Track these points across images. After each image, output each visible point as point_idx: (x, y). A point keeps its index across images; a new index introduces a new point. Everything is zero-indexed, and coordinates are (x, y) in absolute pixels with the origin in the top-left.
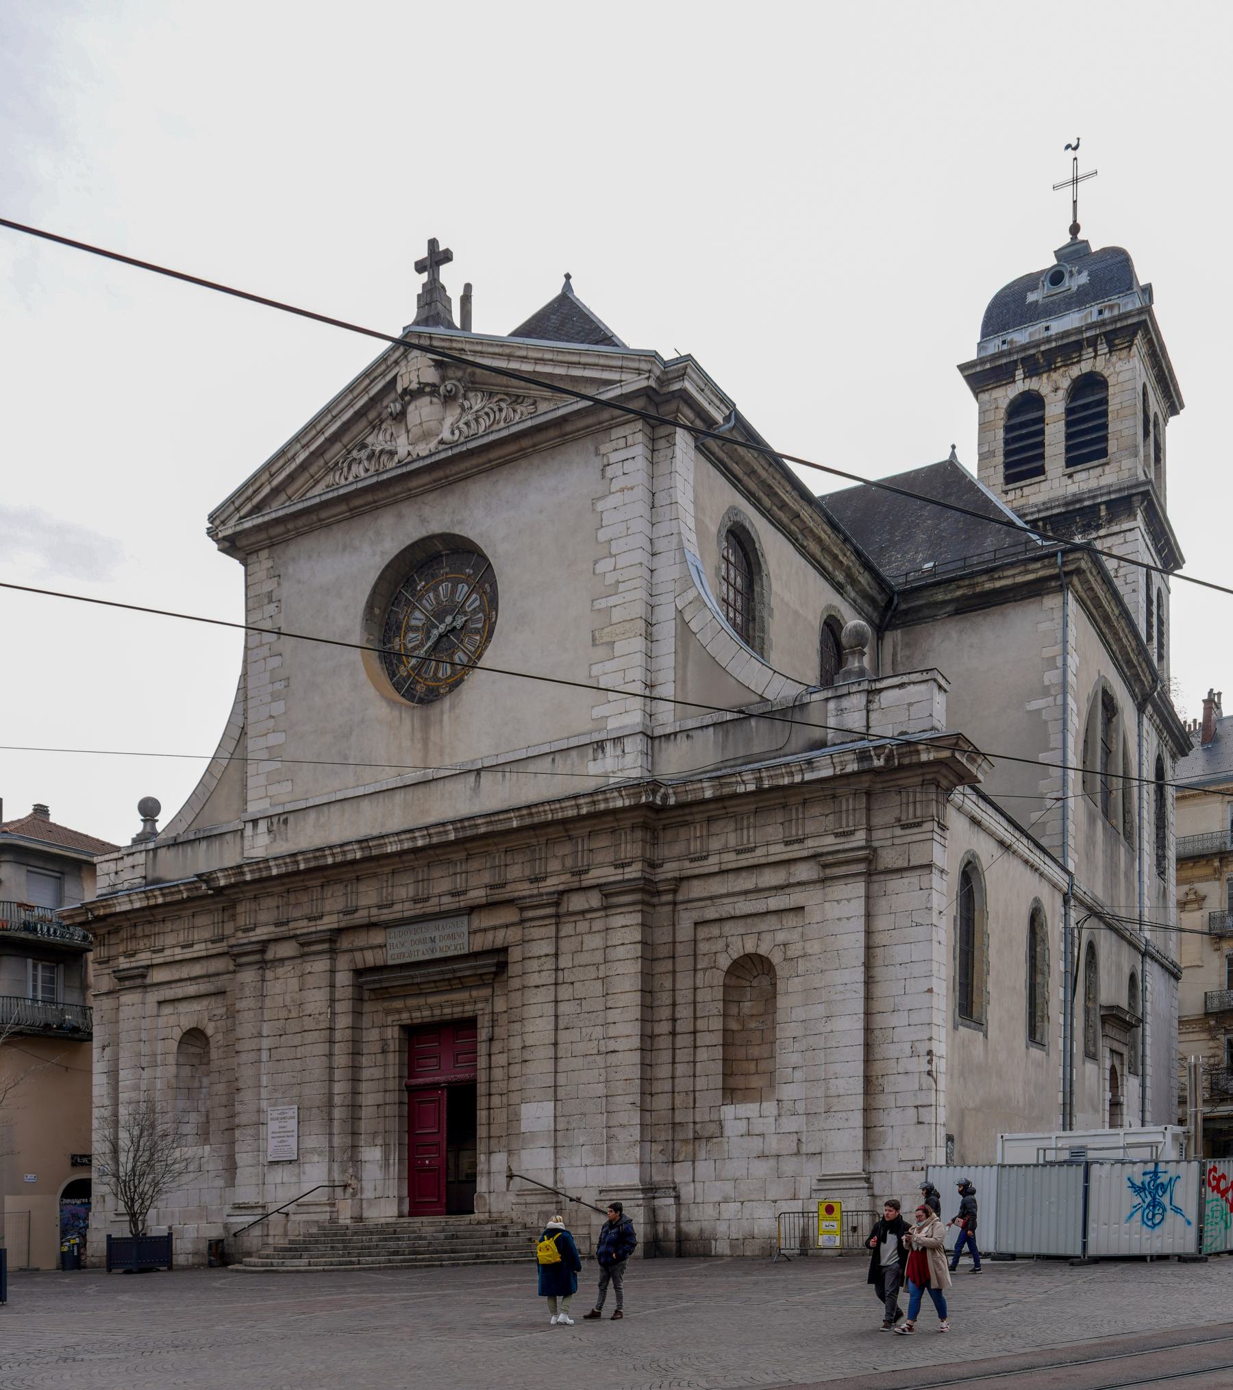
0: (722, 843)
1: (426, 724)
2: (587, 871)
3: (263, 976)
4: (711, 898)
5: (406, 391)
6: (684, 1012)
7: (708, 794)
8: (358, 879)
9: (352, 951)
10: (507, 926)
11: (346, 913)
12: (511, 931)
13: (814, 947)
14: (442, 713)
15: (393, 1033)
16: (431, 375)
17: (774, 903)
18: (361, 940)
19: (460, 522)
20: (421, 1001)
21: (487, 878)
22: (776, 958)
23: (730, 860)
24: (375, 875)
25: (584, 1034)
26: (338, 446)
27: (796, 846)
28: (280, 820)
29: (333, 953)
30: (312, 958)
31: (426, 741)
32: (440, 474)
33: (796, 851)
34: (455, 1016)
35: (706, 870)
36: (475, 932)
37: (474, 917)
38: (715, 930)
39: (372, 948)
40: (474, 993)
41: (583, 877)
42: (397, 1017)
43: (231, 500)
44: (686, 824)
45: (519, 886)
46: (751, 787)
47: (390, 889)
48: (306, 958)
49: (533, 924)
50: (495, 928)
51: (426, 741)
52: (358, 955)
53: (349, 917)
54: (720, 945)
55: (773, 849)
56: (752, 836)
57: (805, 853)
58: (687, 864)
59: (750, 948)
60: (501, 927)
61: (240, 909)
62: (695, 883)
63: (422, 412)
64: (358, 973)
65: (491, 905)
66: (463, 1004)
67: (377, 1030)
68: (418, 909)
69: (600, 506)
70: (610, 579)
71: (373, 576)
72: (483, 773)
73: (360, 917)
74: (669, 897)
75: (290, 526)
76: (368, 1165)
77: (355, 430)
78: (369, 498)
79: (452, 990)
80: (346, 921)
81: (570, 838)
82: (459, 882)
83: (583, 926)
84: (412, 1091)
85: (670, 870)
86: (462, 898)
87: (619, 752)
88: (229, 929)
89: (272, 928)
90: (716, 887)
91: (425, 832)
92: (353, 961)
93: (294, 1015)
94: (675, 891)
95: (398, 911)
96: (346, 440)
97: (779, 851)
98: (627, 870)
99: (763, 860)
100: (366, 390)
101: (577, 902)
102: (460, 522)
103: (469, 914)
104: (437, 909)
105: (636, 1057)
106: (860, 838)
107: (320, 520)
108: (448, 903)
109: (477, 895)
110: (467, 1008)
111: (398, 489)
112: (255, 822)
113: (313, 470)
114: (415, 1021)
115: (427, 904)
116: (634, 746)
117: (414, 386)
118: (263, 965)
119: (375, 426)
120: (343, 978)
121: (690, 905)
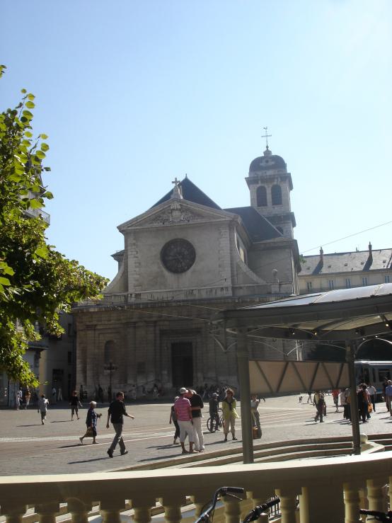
28: (138, 296)
63: (176, 214)
112: (131, 294)
120: (158, 332)
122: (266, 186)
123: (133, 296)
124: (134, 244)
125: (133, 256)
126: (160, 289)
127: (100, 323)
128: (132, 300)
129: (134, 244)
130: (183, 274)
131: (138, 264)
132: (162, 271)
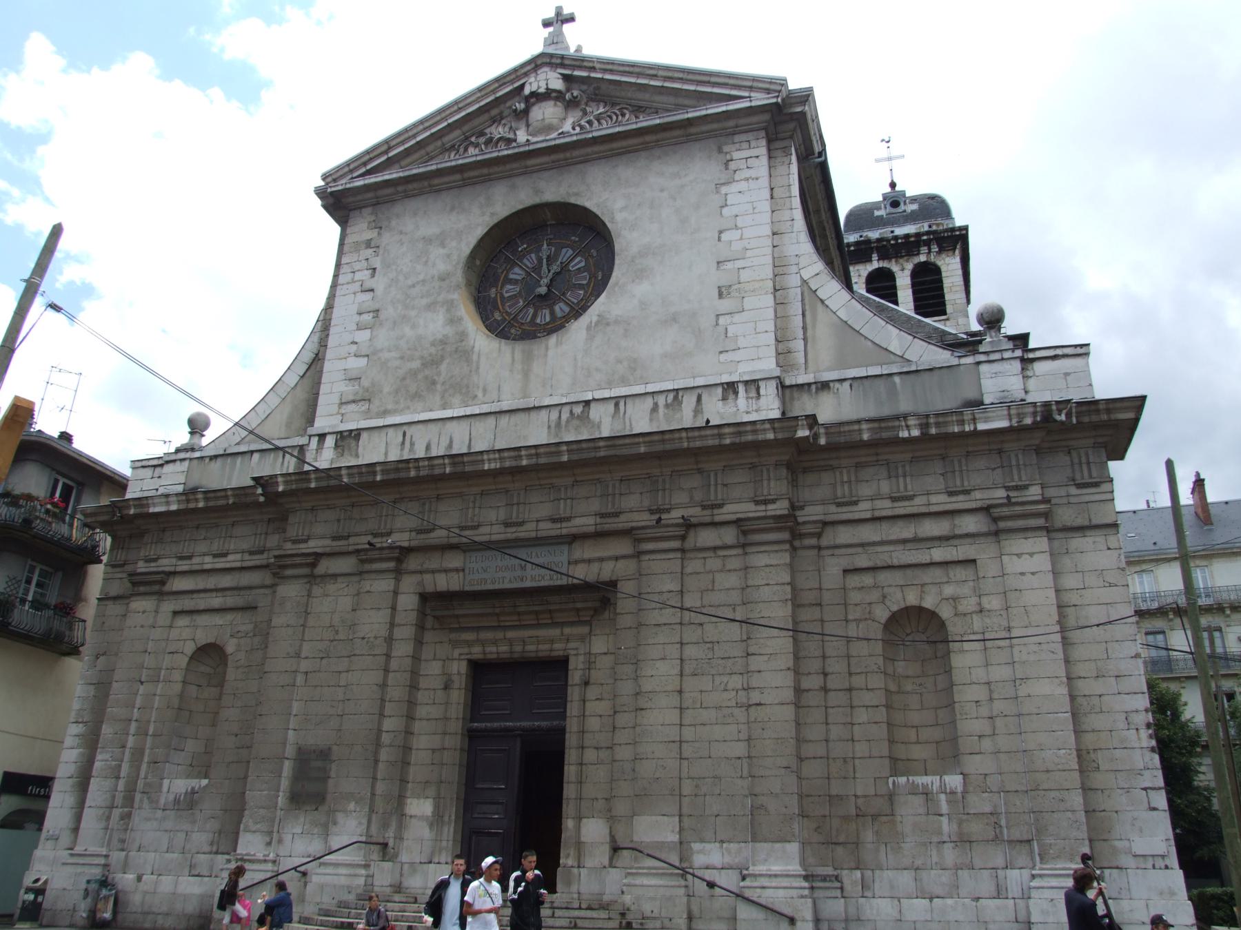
0: (874, 491)
1: (528, 358)
2: (720, 506)
3: (310, 591)
4: (862, 545)
5: (533, 94)
6: (835, 666)
7: (866, 437)
8: (438, 498)
9: (421, 572)
10: (617, 558)
11: (419, 532)
12: (621, 564)
13: (993, 603)
14: (547, 349)
15: (459, 668)
16: (557, 84)
17: (938, 554)
18: (434, 562)
19: (577, 194)
20: (500, 635)
21: (595, 505)
22: (945, 613)
23: (885, 507)
24: (461, 495)
25: (717, 682)
26: (457, 133)
27: (961, 498)
29: (398, 573)
30: (373, 576)
31: (526, 374)
32: (561, 156)
33: (960, 502)
34: (540, 654)
35: (857, 516)
36: (576, 562)
37: (576, 545)
38: (867, 580)
39: (446, 571)
40: (567, 630)
41: (716, 511)
42: (466, 650)
43: (348, 164)
44: (832, 468)
45: (636, 516)
46: (916, 433)
47: (477, 510)
48: (366, 576)
49: (653, 557)
50: (601, 560)
51: (526, 374)
52: (428, 578)
53: (422, 536)
54: (875, 596)
55: (934, 499)
56: (912, 486)
57: (973, 505)
58: (833, 508)
59: (912, 599)
60: (610, 558)
61: (292, 519)
62: (841, 528)
64: (424, 598)
65: (599, 535)
66: (552, 641)
67: (440, 663)
68: (511, 533)
69: (724, 190)
70: (737, 246)
71: (480, 232)
72: (593, 405)
73: (439, 536)
74: (813, 541)
75: (400, 188)
76: (413, 820)
77: (476, 122)
78: (485, 171)
79: (538, 626)
80: (417, 541)
81: (700, 471)
82: (563, 509)
83: (714, 563)
84: (472, 736)
85: (812, 513)
86: (564, 525)
87: (753, 394)
88: (273, 541)
89: (328, 542)
90: (868, 533)
91: (533, 451)
92: (421, 583)
93: (341, 636)
94: (819, 536)
95: (482, 535)
96: (466, 128)
97: (941, 501)
98: (770, 507)
99: (924, 510)
100: (494, 91)
101: (706, 537)
102: (577, 194)
103: (570, 543)
104: (533, 535)
105: (789, 712)
106: (1034, 492)
107: (430, 186)
108: (547, 529)
109: (585, 523)
110: (556, 646)
111: (515, 165)
112: (322, 437)
113: (430, 148)
114: (489, 656)
115: (520, 529)
116: (769, 392)
117: (542, 90)
118: (312, 578)
119: (496, 120)
120: (408, 601)
121: (837, 552)
122: (894, 267)
123: (330, 441)
124: (368, 244)
125: (357, 287)
126: (444, 407)
127: (184, 566)
128: (325, 458)
129: (368, 244)
130: (553, 339)
131: (367, 318)
132: (462, 336)
